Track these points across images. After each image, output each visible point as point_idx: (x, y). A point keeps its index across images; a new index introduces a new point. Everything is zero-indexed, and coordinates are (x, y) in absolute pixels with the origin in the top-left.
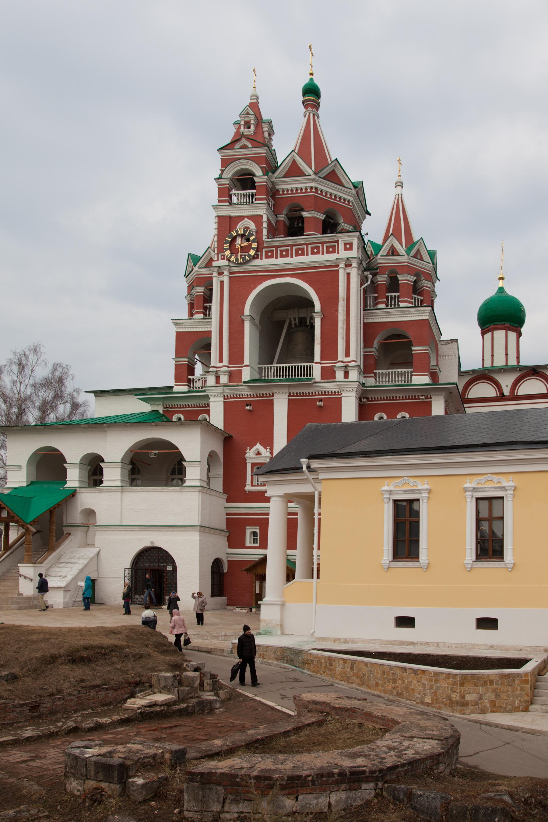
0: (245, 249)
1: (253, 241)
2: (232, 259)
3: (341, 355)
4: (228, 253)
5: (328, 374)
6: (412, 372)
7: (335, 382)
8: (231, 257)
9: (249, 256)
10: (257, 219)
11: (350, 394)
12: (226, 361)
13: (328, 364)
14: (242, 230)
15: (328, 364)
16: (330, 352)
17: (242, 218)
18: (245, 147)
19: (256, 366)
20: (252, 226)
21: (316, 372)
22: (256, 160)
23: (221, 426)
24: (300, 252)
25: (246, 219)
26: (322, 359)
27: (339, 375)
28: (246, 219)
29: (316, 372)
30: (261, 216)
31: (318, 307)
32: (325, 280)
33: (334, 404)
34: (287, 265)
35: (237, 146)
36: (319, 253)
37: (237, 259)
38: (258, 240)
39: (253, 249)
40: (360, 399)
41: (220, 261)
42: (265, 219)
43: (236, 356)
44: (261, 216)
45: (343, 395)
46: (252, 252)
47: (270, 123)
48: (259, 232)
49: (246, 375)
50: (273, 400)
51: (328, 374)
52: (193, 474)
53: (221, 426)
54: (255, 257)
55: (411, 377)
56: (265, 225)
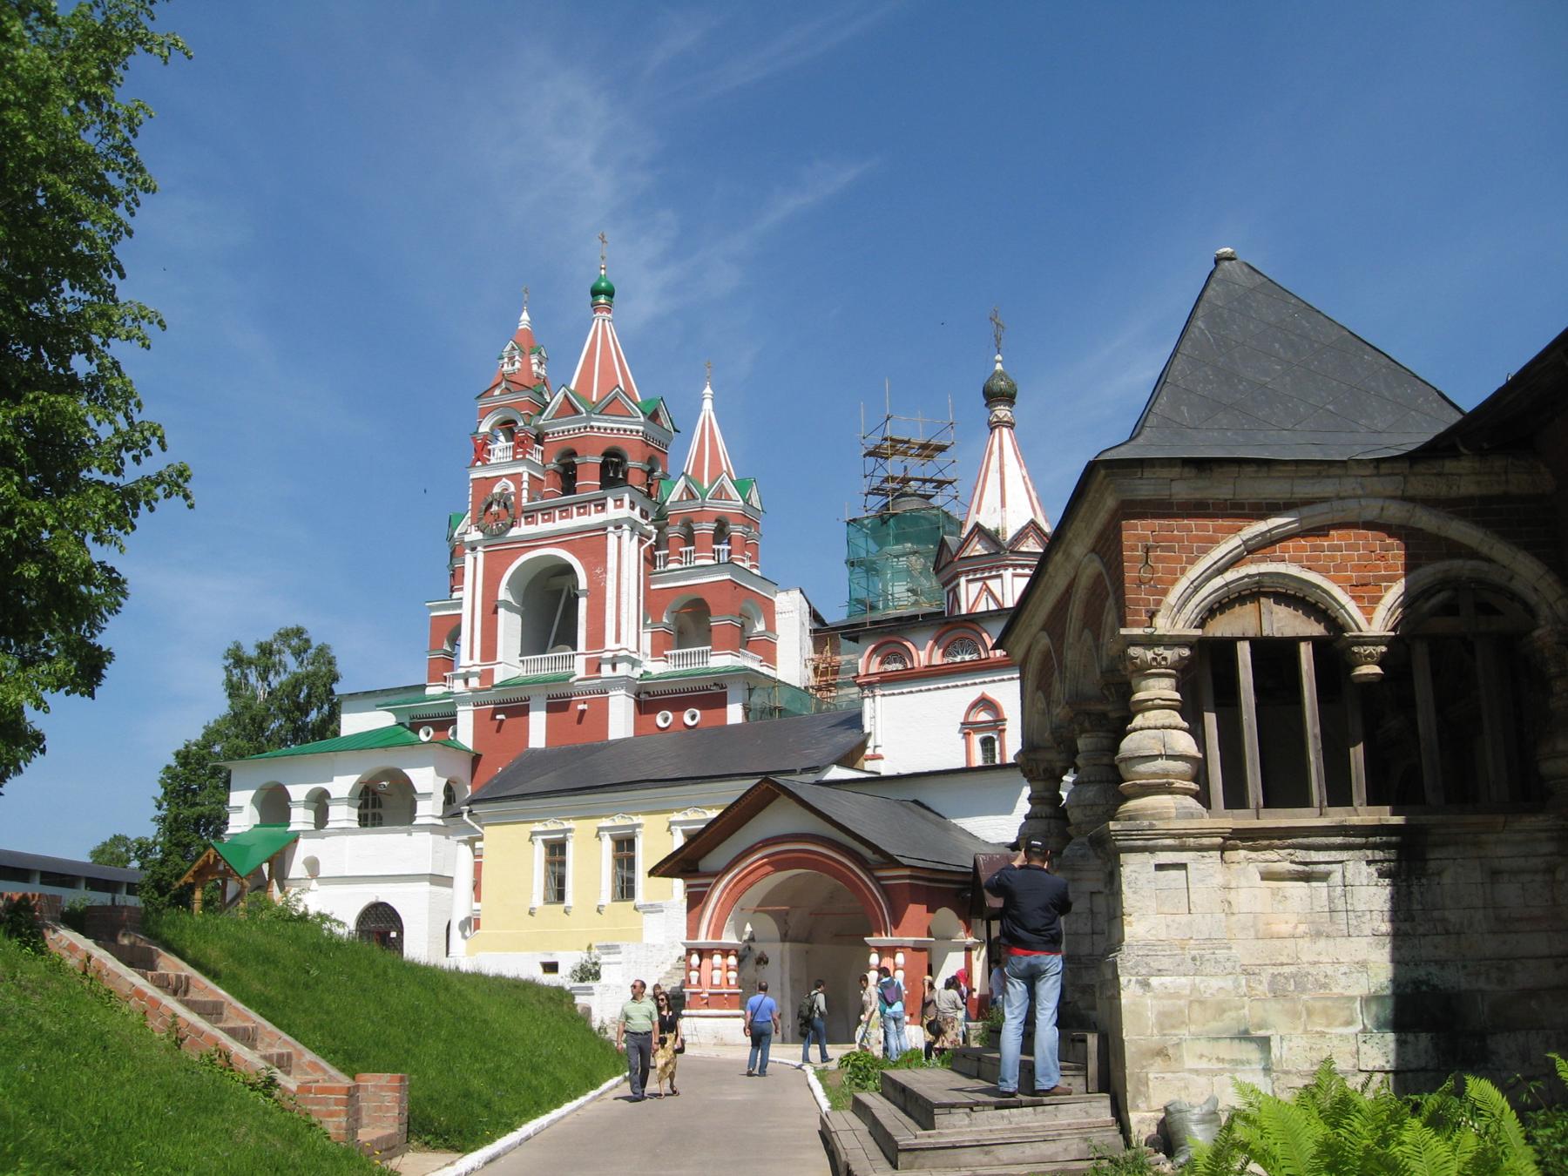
0: (497, 517)
3: (610, 643)
10: (516, 478)
12: (477, 659)
16: (596, 640)
17: (498, 478)
20: (512, 488)
23: (470, 745)
26: (588, 647)
27: (606, 670)
30: (520, 474)
31: (583, 584)
34: (544, 535)
35: (497, 392)
40: (638, 695)
42: (525, 477)
44: (520, 474)
46: (509, 521)
48: (518, 494)
51: (595, 666)
52: (429, 809)
53: (470, 745)
56: (525, 485)
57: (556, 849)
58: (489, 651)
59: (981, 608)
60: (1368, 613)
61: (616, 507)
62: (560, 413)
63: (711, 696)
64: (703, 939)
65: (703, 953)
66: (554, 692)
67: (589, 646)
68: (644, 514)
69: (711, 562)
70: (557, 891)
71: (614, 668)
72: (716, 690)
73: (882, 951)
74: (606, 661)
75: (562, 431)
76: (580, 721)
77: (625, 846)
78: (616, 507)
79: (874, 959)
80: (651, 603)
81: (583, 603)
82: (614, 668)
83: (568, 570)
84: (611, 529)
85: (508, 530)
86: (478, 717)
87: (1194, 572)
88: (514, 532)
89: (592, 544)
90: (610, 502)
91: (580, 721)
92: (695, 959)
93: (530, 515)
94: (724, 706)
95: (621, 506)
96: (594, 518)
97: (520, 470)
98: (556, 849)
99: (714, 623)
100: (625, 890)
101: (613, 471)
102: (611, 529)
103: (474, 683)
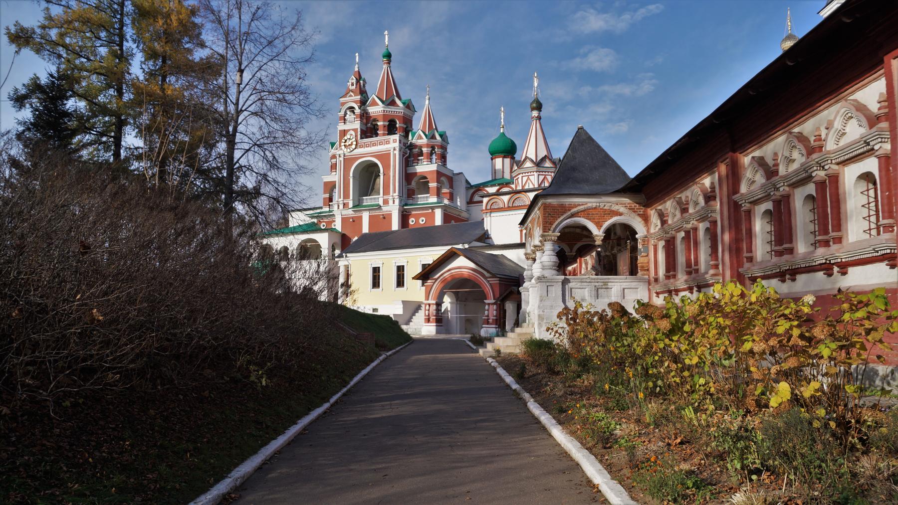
5: (386, 202)
10: (355, 130)
13: (386, 197)
15: (386, 197)
16: (386, 192)
18: (351, 96)
19: (357, 199)
20: (353, 133)
21: (381, 202)
22: (355, 102)
23: (340, 230)
24: (374, 145)
27: (391, 202)
32: (385, 157)
33: (387, 218)
43: (346, 196)
47: (364, 81)
49: (351, 205)
51: (386, 202)
57: (376, 271)
58: (346, 196)
59: (526, 187)
60: (599, 229)
64: (430, 302)
65: (429, 305)
68: (405, 144)
70: (376, 283)
73: (489, 304)
77: (400, 269)
79: (487, 307)
80: (408, 177)
83: (376, 165)
87: (559, 220)
90: (391, 141)
92: (427, 307)
98: (376, 271)
99: (431, 185)
100: (400, 282)
101: (391, 129)
103: (341, 206)
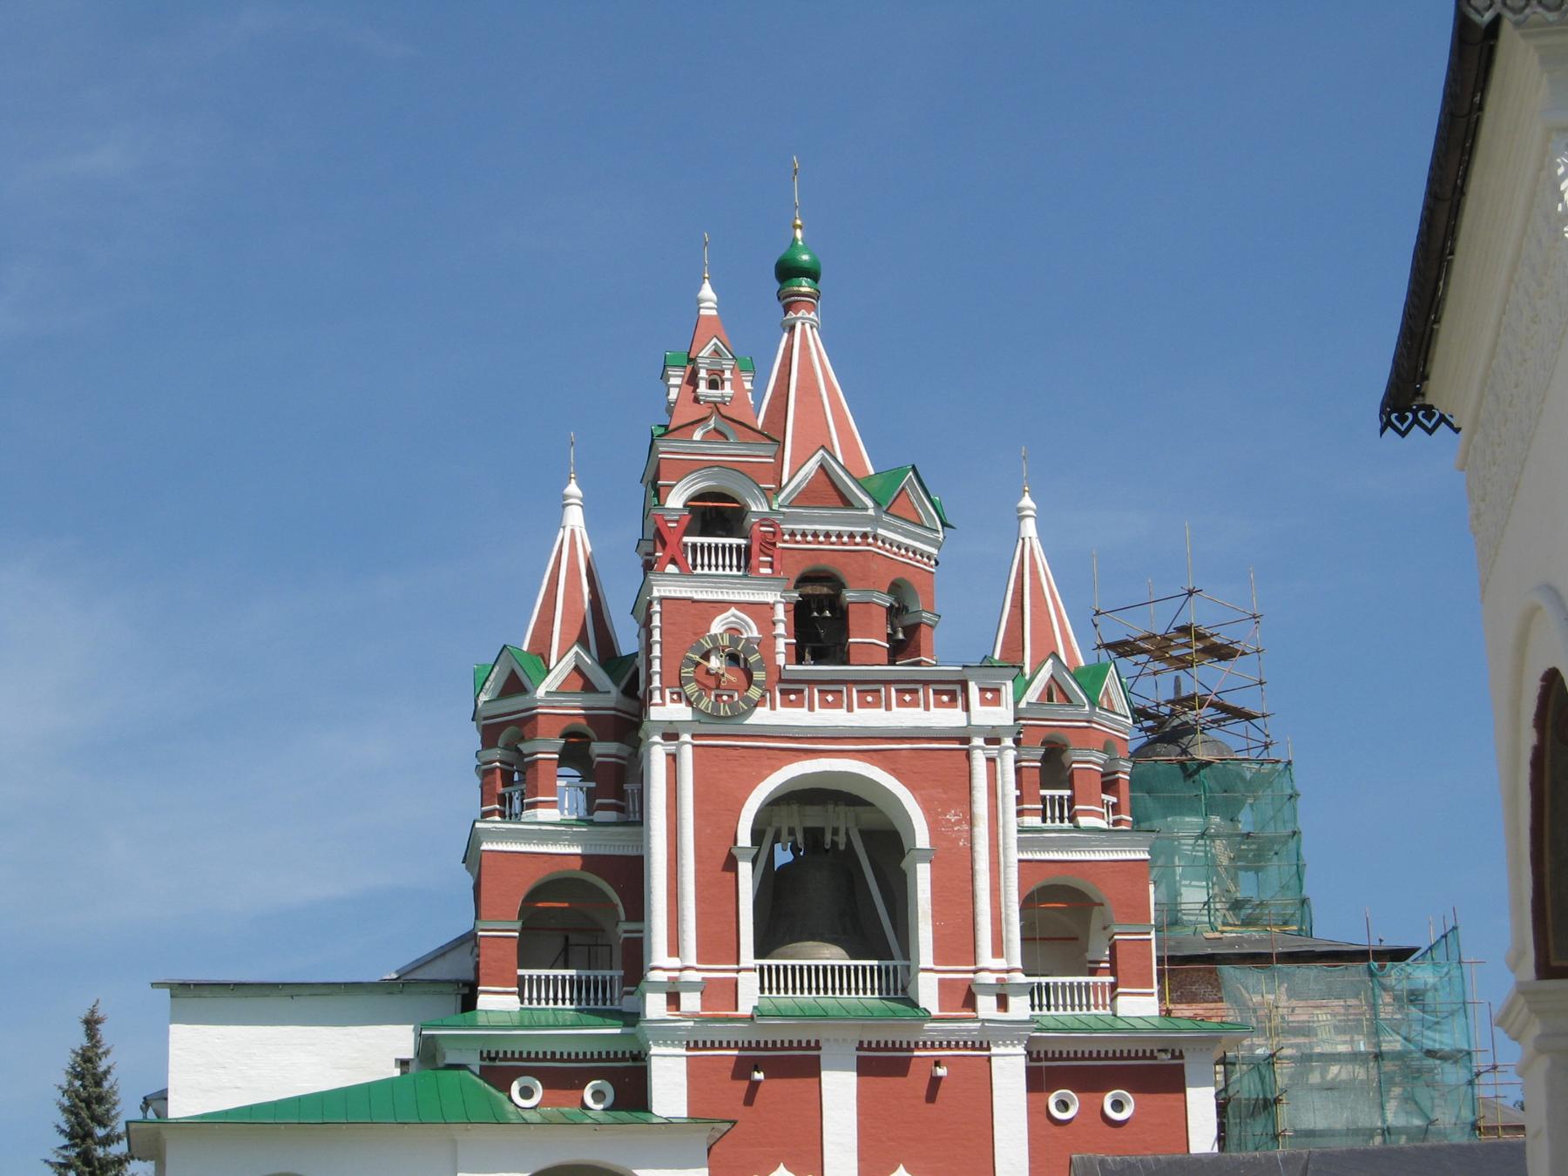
1: (760, 665)
2: (702, 706)
4: (691, 688)
6: (1114, 986)
7: (975, 1019)
8: (700, 698)
9: (747, 700)
10: (760, 611)
11: (1010, 1050)
14: (726, 637)
15: (959, 973)
17: (723, 605)
25: (733, 610)
27: (986, 1006)
28: (733, 610)
29: (928, 992)
30: (772, 607)
36: (918, 705)
37: (716, 707)
38: (768, 660)
39: (758, 685)
41: (669, 705)
42: (780, 613)
44: (772, 607)
45: (994, 1050)
50: (818, 1057)
54: (759, 703)
55: (1113, 999)
61: (984, 702)
62: (807, 497)
63: (1157, 1073)
66: (873, 1037)
67: (940, 955)
69: (1103, 824)
71: (1003, 1003)
72: (1164, 1058)
74: (987, 989)
75: (819, 533)
76: (931, 1096)
78: (984, 702)
81: (923, 876)
82: (1003, 1003)
84: (978, 741)
85: (749, 712)
86: (697, 1074)
88: (761, 716)
89: (941, 765)
91: (931, 1096)
93: (792, 690)
94: (1181, 1089)
95: (996, 702)
96: (948, 718)
97: (770, 597)
102: (978, 741)
